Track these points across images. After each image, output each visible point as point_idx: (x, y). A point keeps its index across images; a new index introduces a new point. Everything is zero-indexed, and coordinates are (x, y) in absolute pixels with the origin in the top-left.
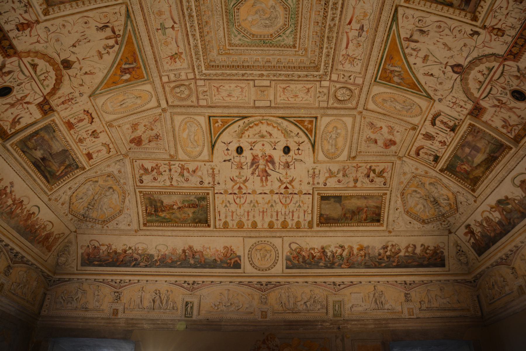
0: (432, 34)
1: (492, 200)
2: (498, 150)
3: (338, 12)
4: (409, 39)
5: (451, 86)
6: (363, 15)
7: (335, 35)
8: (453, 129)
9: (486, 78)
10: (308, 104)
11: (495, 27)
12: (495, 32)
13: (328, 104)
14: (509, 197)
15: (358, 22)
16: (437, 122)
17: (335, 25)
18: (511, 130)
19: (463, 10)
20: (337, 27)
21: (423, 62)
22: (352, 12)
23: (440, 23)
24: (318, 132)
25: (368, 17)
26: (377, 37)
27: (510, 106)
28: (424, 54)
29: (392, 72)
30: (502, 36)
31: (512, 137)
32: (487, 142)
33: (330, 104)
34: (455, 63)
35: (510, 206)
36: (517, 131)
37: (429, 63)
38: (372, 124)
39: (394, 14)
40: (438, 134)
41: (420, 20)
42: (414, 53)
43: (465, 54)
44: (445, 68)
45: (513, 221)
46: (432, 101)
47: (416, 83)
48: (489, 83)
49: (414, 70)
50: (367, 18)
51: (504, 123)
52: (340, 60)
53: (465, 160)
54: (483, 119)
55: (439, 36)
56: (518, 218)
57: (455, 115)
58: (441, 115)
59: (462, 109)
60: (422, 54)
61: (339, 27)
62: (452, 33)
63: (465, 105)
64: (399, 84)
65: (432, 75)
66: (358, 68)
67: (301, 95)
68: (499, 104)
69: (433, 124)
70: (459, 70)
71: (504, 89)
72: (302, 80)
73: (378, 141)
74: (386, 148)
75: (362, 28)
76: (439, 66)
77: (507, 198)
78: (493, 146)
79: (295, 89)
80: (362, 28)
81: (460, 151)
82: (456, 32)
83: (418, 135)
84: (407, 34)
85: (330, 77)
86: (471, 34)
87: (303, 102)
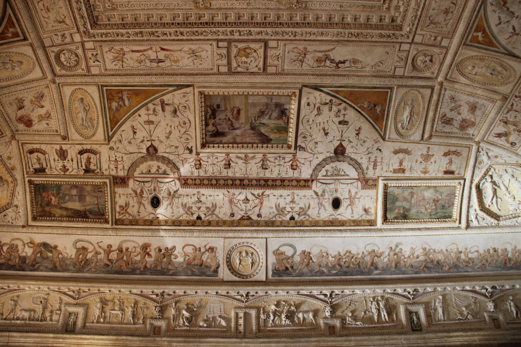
0: (176, 119)
1: (39, 238)
2: (96, 215)
3: (173, 37)
4: (163, 104)
5: (132, 151)
6: (175, 59)
7: (145, 38)
8: (87, 171)
9: (155, 174)
10: (42, 26)
11: (201, 161)
12: (198, 163)
13: (50, 46)
14: (58, 249)
15: (167, 57)
16: (85, 155)
17: (159, 37)
18: (122, 214)
19: (206, 135)
20: (156, 38)
21: (144, 122)
22: (176, 49)
23: (188, 122)
24: (5, 46)
25: (174, 64)
26: (156, 76)
27: (143, 201)
28: (153, 120)
29: (122, 99)
30: (196, 169)
31: (117, 217)
32: (96, 202)
33: (49, 50)
34: (156, 146)
35: (50, 255)
36: (124, 218)
37: (147, 127)
38: (42, 97)
39: (184, 85)
40: (72, 161)
41: (185, 107)
42: (151, 112)
43: (168, 150)
44: (147, 141)
45: (39, 266)
46: (107, 142)
47: (120, 123)
48: (153, 177)
49: (132, 117)
50: (173, 64)
51: (124, 205)
52: (115, 48)
53: (61, 195)
54: (116, 189)
55: (176, 126)
56: (46, 267)
57: (105, 166)
58: (96, 155)
59: (115, 169)
60: (152, 118)
61: (156, 40)
62: (183, 134)
63: (121, 170)
64: (110, 108)
65: (135, 133)
66: (110, 66)
67: (52, 15)
68: (138, 193)
69: (81, 153)
70: (151, 152)
71: (154, 190)
72: (73, 13)
73: (23, 110)
74: (17, 120)
75: (161, 61)
76: (146, 135)
77: (55, 247)
78: (96, 209)
79: (57, 6)
80: (161, 61)
81: (68, 187)
82: (185, 136)
83: (57, 144)
84: (168, 100)
85: (88, 41)
86: (188, 147)
87: (42, 20)
